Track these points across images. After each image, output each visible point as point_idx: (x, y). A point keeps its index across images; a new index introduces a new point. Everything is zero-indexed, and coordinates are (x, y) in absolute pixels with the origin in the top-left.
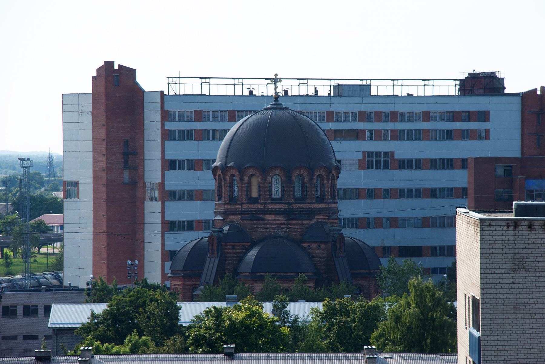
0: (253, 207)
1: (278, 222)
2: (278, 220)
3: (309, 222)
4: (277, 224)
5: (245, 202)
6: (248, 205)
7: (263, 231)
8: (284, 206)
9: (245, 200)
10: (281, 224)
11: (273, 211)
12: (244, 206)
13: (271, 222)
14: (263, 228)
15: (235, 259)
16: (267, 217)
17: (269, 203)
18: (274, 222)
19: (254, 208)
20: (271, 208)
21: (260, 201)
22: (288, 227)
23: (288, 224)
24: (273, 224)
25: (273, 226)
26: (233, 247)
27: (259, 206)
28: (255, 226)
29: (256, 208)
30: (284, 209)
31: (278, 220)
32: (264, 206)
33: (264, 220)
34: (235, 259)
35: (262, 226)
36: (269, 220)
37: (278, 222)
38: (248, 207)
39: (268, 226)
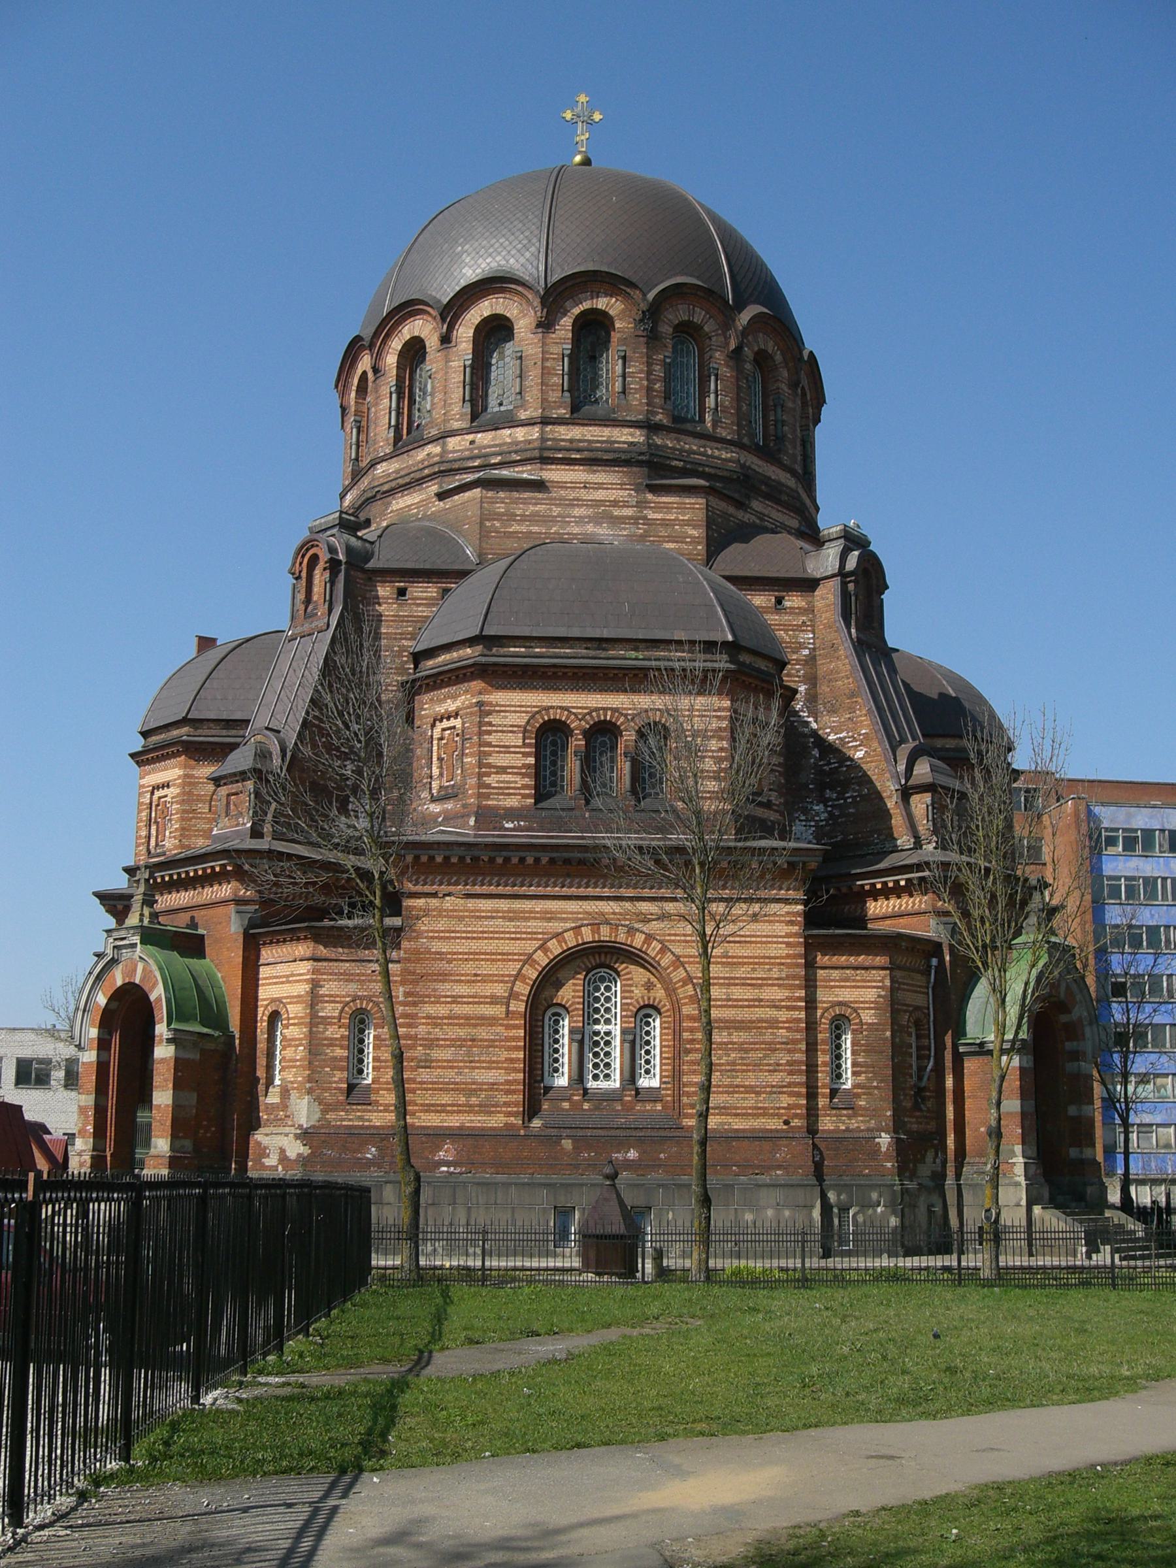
0: (493, 439)
1: (600, 495)
2: (600, 486)
3: (731, 510)
4: (601, 503)
5: (456, 425)
6: (470, 437)
7: (535, 529)
8: (626, 436)
9: (457, 420)
10: (615, 503)
11: (578, 450)
12: (452, 443)
13: (572, 495)
14: (533, 518)
15: (405, 643)
16: (553, 474)
17: (560, 421)
18: (584, 494)
19: (496, 446)
20: (571, 441)
21: (523, 415)
22: (645, 518)
23: (642, 505)
24: (576, 502)
25: (577, 512)
26: (402, 592)
27: (520, 434)
28: (501, 508)
29: (505, 444)
30: (624, 443)
31: (600, 486)
32: (542, 432)
33: (539, 486)
34: (405, 643)
35: (532, 508)
36: (562, 485)
37: (600, 495)
38: (472, 442)
39: (556, 511)
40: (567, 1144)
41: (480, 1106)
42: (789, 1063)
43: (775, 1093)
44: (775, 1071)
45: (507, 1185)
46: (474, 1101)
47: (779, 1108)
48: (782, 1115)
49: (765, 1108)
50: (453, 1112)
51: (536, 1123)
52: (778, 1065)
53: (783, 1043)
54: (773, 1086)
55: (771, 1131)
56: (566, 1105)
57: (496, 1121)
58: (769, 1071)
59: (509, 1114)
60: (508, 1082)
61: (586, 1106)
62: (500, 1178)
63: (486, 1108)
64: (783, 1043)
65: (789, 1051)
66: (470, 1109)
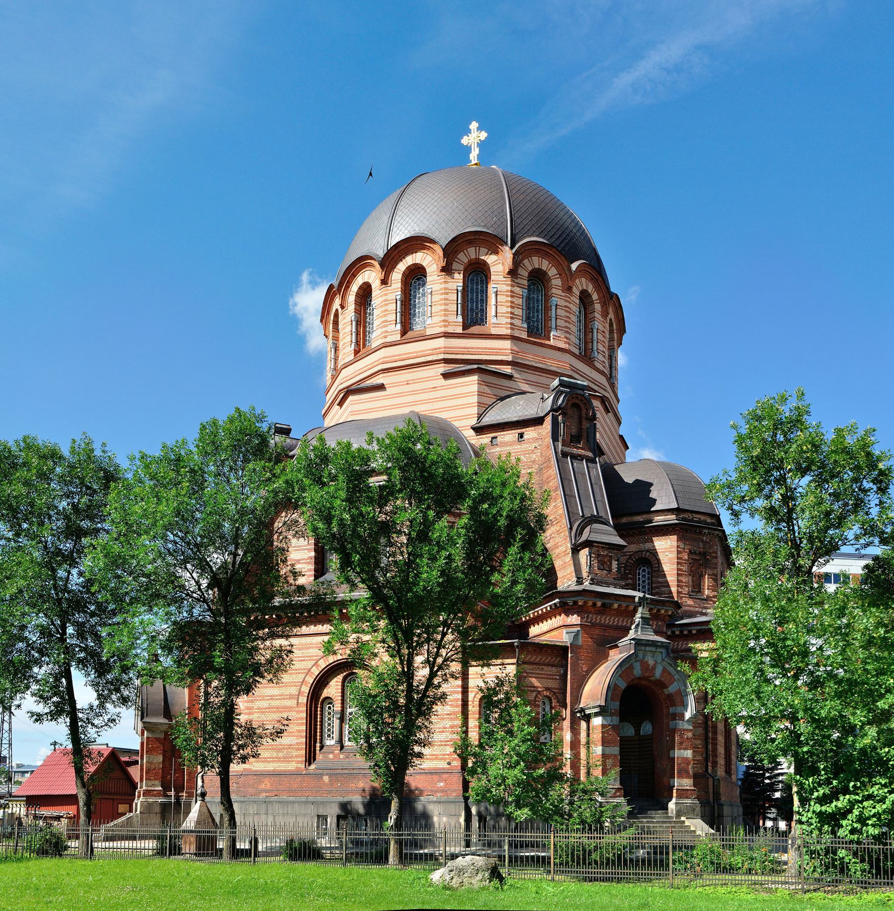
40: (326, 779)
41: (284, 758)
42: (451, 727)
43: (442, 745)
44: (443, 732)
45: (293, 802)
46: (281, 755)
47: (444, 755)
48: (447, 759)
49: (437, 755)
50: (271, 762)
51: (313, 767)
52: (445, 728)
53: (448, 714)
54: (441, 741)
55: (440, 769)
56: (331, 756)
57: (291, 766)
58: (440, 732)
59: (298, 762)
60: (298, 744)
61: (342, 756)
62: (291, 799)
63: (286, 759)
64: (448, 714)
65: (452, 719)
66: (279, 760)
